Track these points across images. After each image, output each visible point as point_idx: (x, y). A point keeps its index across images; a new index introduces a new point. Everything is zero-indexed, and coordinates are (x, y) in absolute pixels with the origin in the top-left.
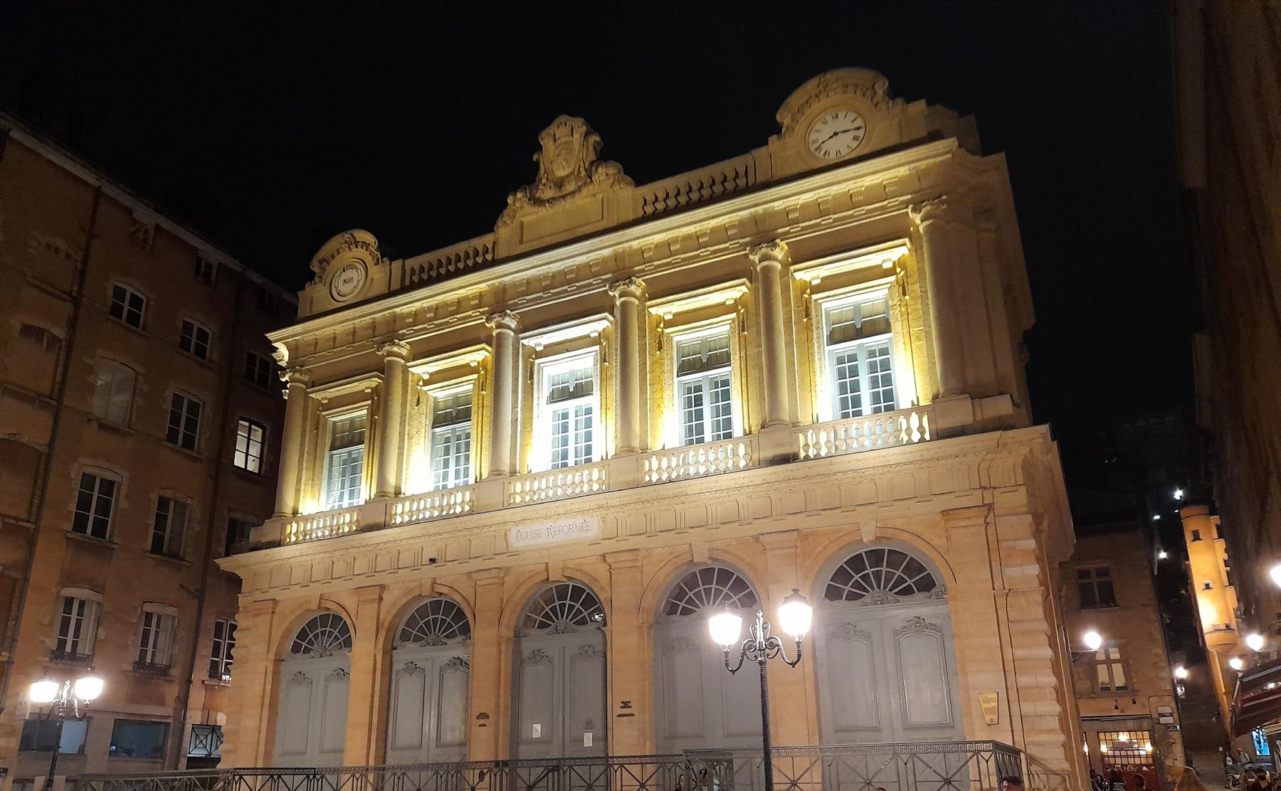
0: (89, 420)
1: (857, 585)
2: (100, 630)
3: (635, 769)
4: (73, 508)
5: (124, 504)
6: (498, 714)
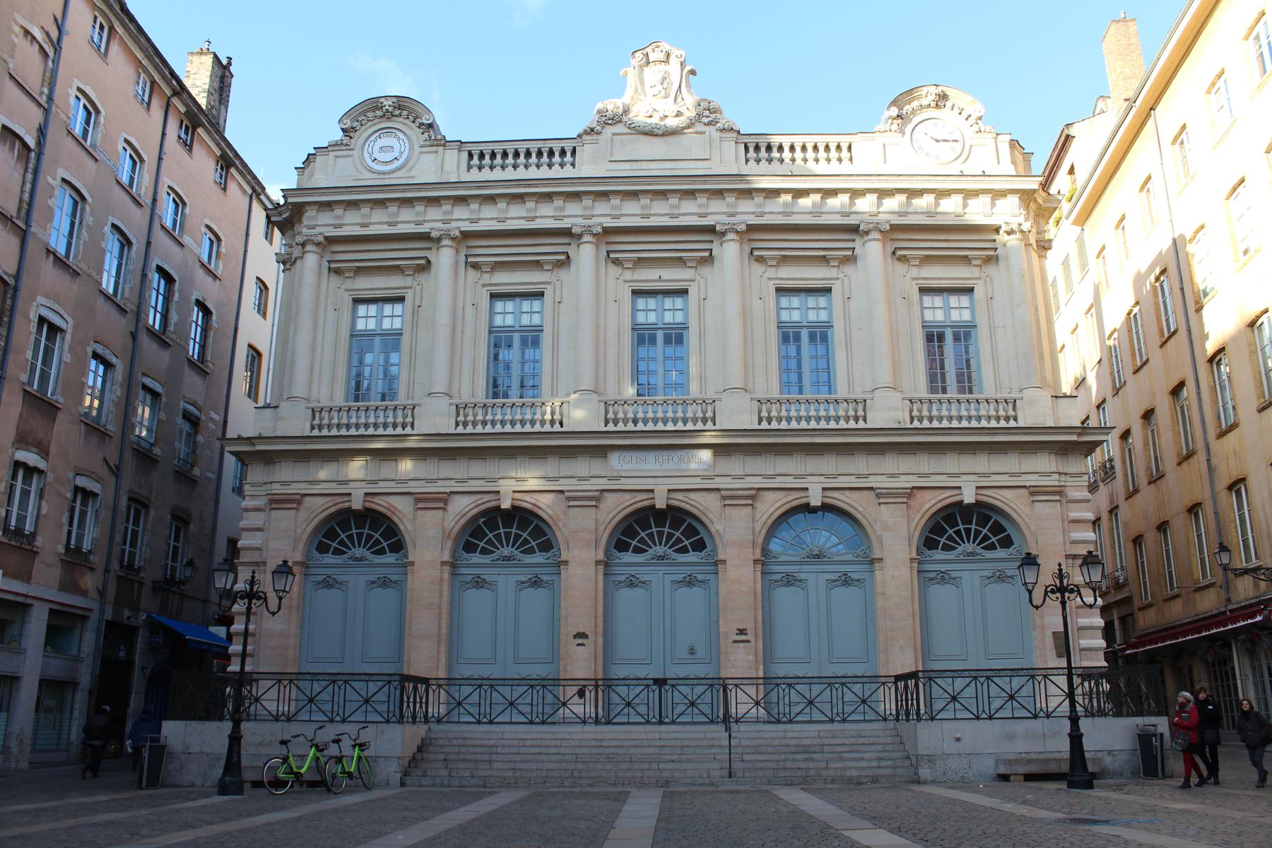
0: (48, 251)
1: (950, 538)
2: (44, 503)
3: (751, 690)
4: (29, 354)
5: (67, 357)
6: (596, 635)
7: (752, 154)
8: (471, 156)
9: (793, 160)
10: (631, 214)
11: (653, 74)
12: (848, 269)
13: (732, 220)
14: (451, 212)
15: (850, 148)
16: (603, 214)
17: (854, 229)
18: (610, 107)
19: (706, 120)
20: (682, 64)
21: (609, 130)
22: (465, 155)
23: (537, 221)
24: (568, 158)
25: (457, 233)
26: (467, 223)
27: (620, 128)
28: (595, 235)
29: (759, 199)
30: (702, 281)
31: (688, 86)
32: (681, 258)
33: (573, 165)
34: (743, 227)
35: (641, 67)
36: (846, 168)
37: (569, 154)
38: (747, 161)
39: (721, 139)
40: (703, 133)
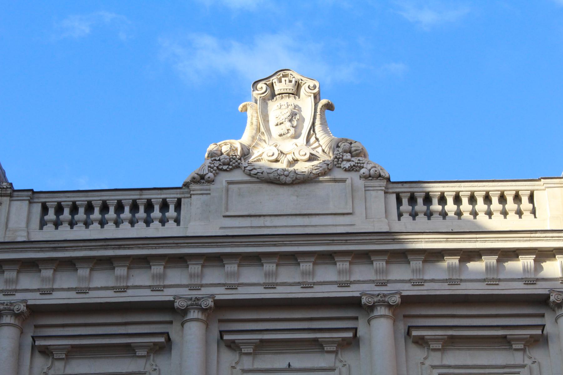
7: (406, 206)
8: (45, 209)
9: (459, 214)
10: (252, 283)
11: (278, 110)
12: (537, 354)
13: (383, 290)
14: (16, 281)
15: (531, 199)
16: (215, 284)
17: (542, 301)
18: (225, 149)
19: (347, 165)
20: (317, 98)
21: (224, 178)
22: (37, 208)
23: (130, 292)
24: (171, 212)
25: (23, 307)
26: (37, 295)
27: (237, 176)
28: (203, 310)
29: (416, 264)
30: (344, 370)
31: (324, 123)
32: (316, 340)
33: (177, 221)
34: (397, 299)
35: (265, 101)
36: (527, 222)
37: (172, 207)
38: (400, 215)
39: (367, 189)
40: (344, 181)
